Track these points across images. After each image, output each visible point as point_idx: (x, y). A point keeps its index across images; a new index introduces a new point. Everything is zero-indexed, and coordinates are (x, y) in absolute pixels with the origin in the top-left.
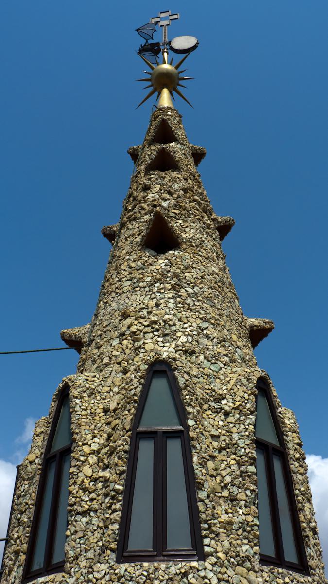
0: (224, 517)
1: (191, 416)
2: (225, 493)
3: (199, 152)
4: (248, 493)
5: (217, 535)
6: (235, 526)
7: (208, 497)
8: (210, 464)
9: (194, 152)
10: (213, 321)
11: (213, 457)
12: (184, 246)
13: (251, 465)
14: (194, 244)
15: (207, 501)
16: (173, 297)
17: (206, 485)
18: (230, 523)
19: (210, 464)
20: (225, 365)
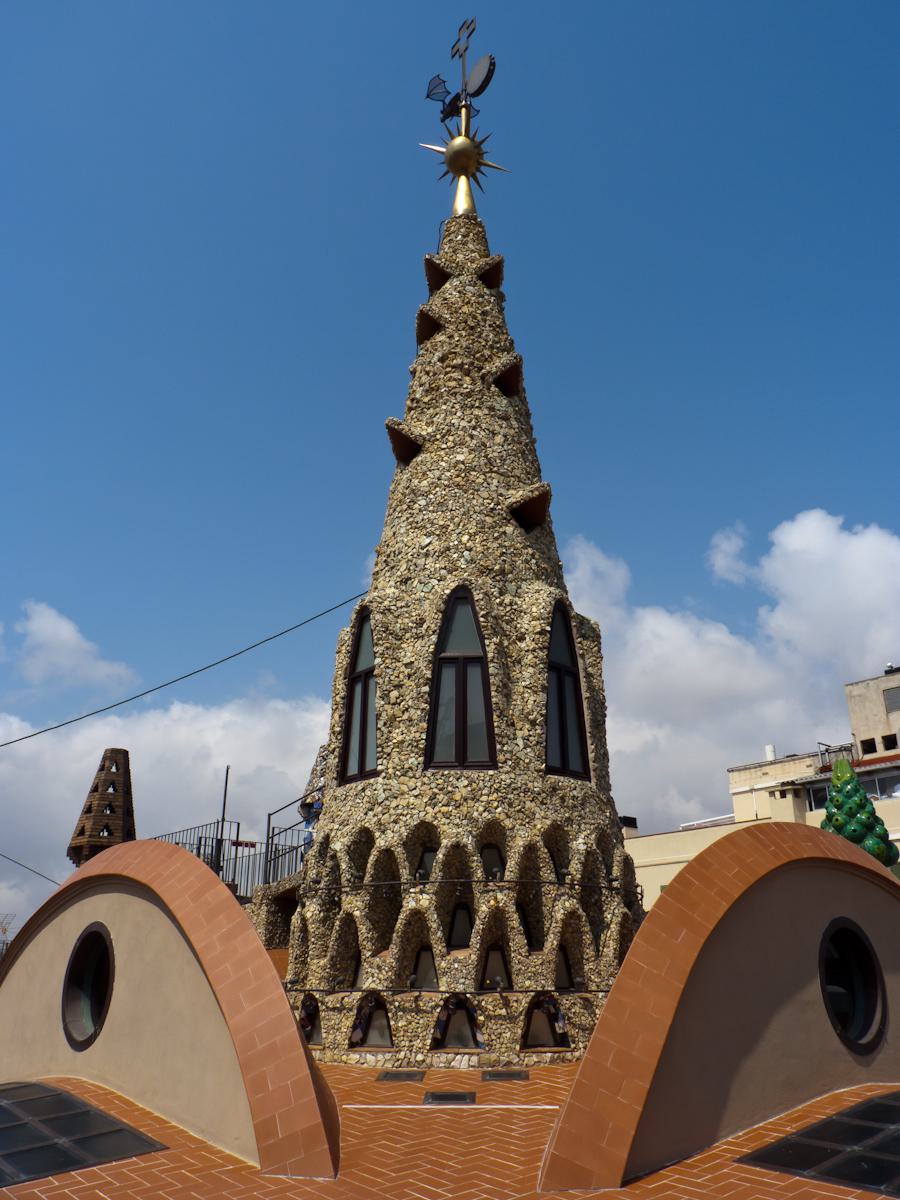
0: (400, 738)
1: (377, 655)
2: (405, 717)
3: (488, 267)
4: (419, 712)
5: (389, 755)
6: (406, 744)
7: (385, 724)
8: (394, 694)
9: (479, 273)
10: (438, 532)
11: (399, 686)
12: (428, 445)
13: (425, 685)
14: (438, 437)
15: (383, 728)
16: (408, 519)
17: (384, 714)
18: (402, 742)
19: (394, 694)
20: (439, 581)
